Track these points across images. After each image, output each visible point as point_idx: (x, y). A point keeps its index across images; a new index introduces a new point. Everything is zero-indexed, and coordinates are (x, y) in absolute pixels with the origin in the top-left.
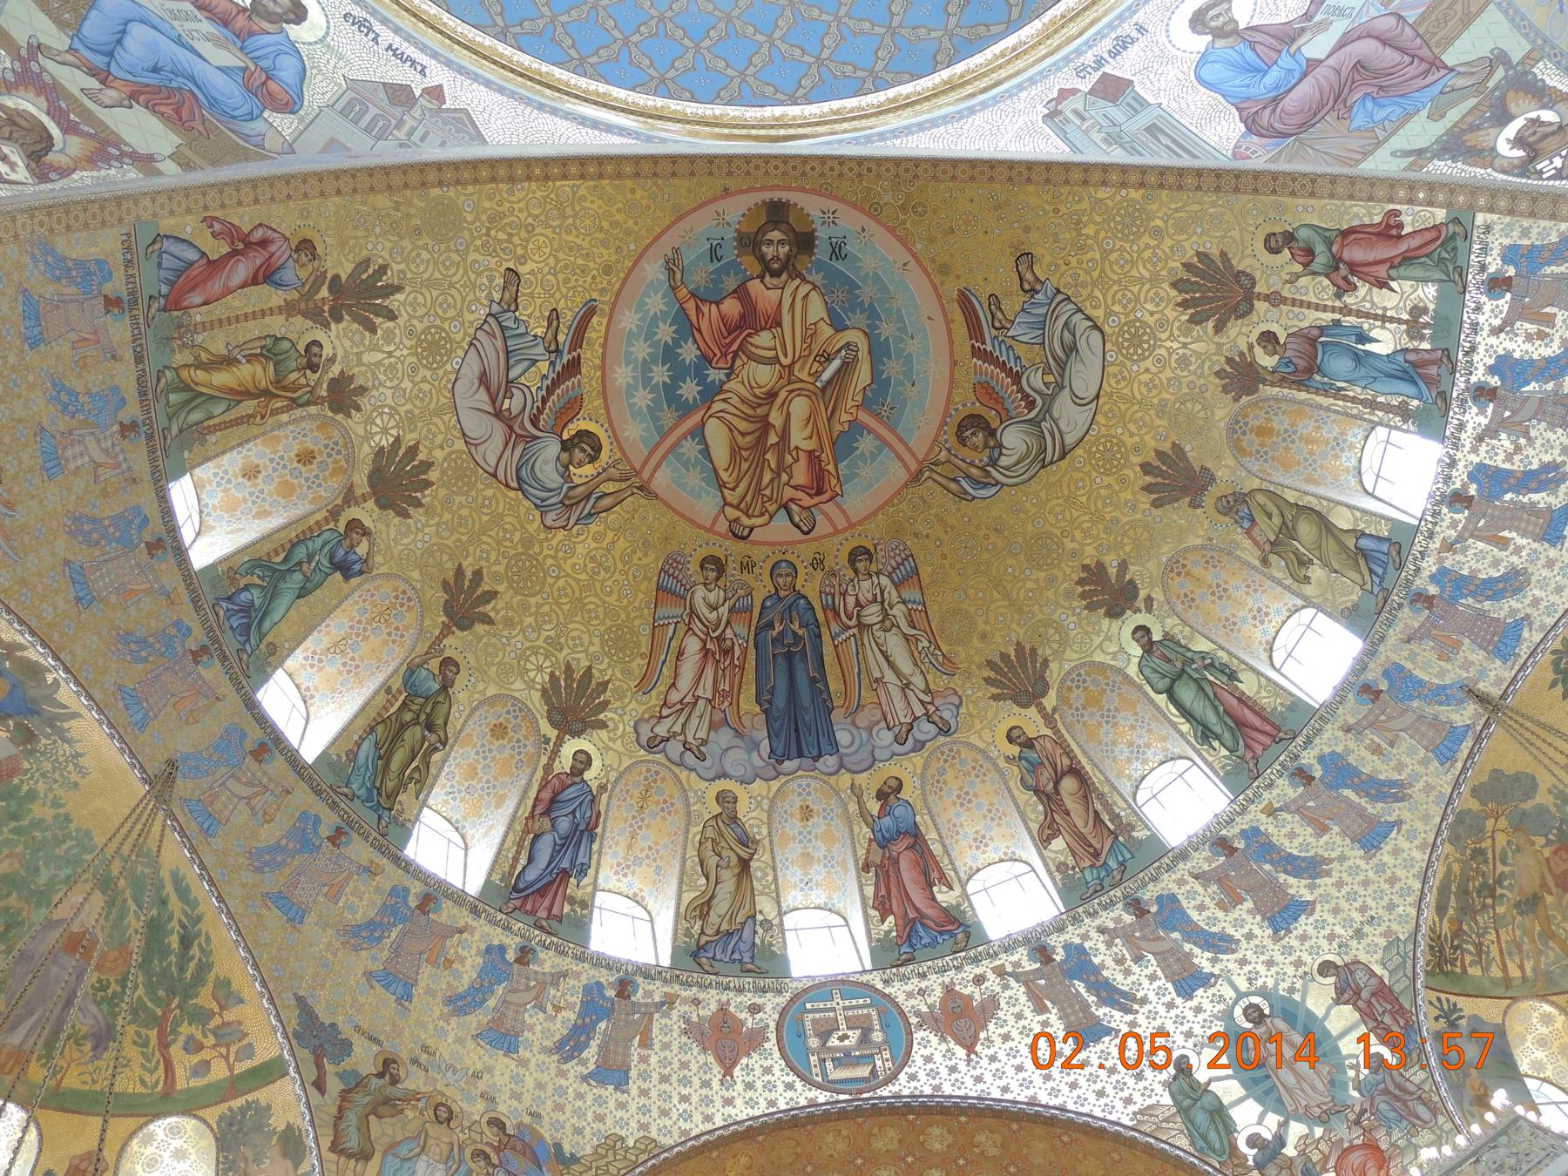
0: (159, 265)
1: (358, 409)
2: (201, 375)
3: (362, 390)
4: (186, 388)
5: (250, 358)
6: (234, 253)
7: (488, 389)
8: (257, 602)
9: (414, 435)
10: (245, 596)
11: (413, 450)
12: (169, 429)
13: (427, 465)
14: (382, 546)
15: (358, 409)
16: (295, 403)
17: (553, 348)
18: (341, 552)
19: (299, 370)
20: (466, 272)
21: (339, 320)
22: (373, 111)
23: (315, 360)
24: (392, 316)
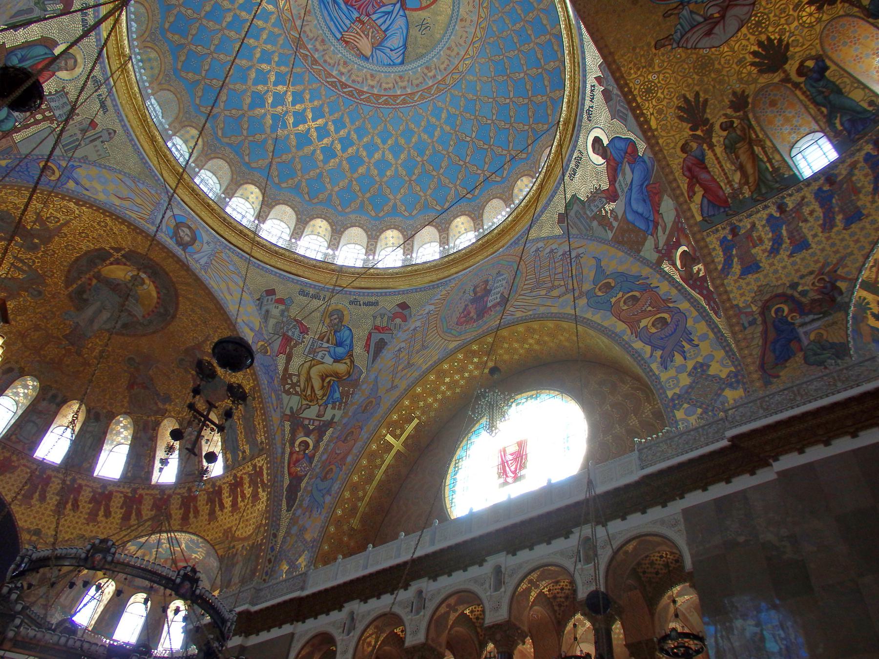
0: (714, 215)
1: (743, 92)
2: (751, 180)
3: (734, 93)
4: (758, 185)
5: (737, 158)
6: (698, 182)
7: (713, 28)
8: (849, 117)
9: (747, 56)
10: (847, 125)
11: (755, 54)
12: (777, 188)
13: (760, 44)
14: (807, 52)
15: (743, 92)
16: (750, 127)
17: (681, 7)
18: (815, 75)
19: (735, 131)
20: (665, 68)
21: (707, 120)
22: (618, 108)
23: (728, 124)
24: (697, 95)
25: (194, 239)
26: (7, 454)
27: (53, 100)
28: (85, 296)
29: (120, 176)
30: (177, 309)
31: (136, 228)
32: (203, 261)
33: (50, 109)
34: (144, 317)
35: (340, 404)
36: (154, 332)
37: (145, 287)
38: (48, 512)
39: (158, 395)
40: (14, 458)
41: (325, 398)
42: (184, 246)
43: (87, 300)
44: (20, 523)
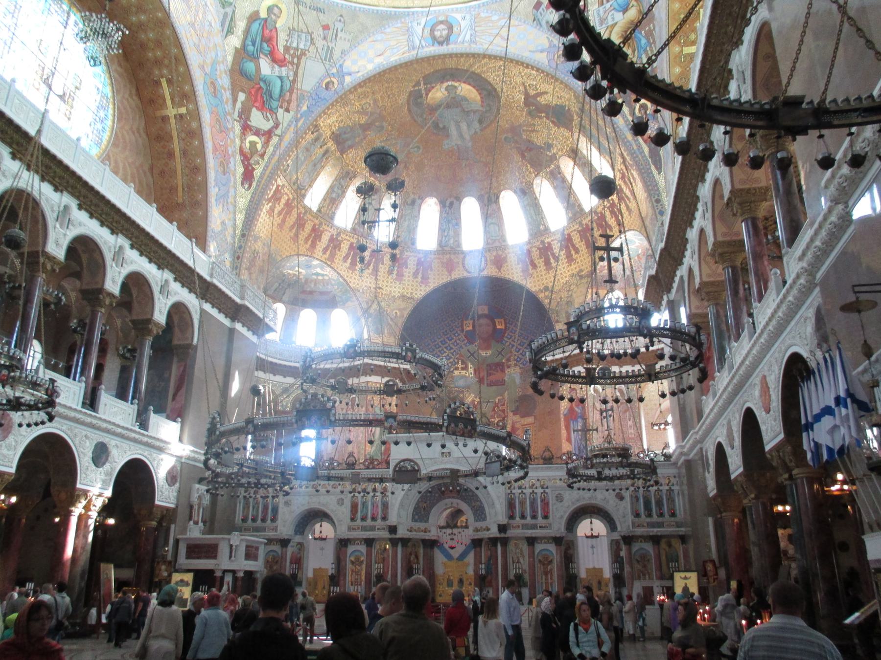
25: (450, 28)
26: (494, 253)
27: (292, 43)
28: (441, 126)
29: (370, 39)
30: (490, 84)
31: (406, 63)
32: (468, 38)
33: (297, 49)
34: (482, 106)
35: (651, 47)
36: (498, 110)
37: (460, 88)
38: (544, 273)
39: (542, 147)
40: (500, 253)
41: (636, 53)
42: (446, 40)
43: (444, 127)
44: (533, 289)
